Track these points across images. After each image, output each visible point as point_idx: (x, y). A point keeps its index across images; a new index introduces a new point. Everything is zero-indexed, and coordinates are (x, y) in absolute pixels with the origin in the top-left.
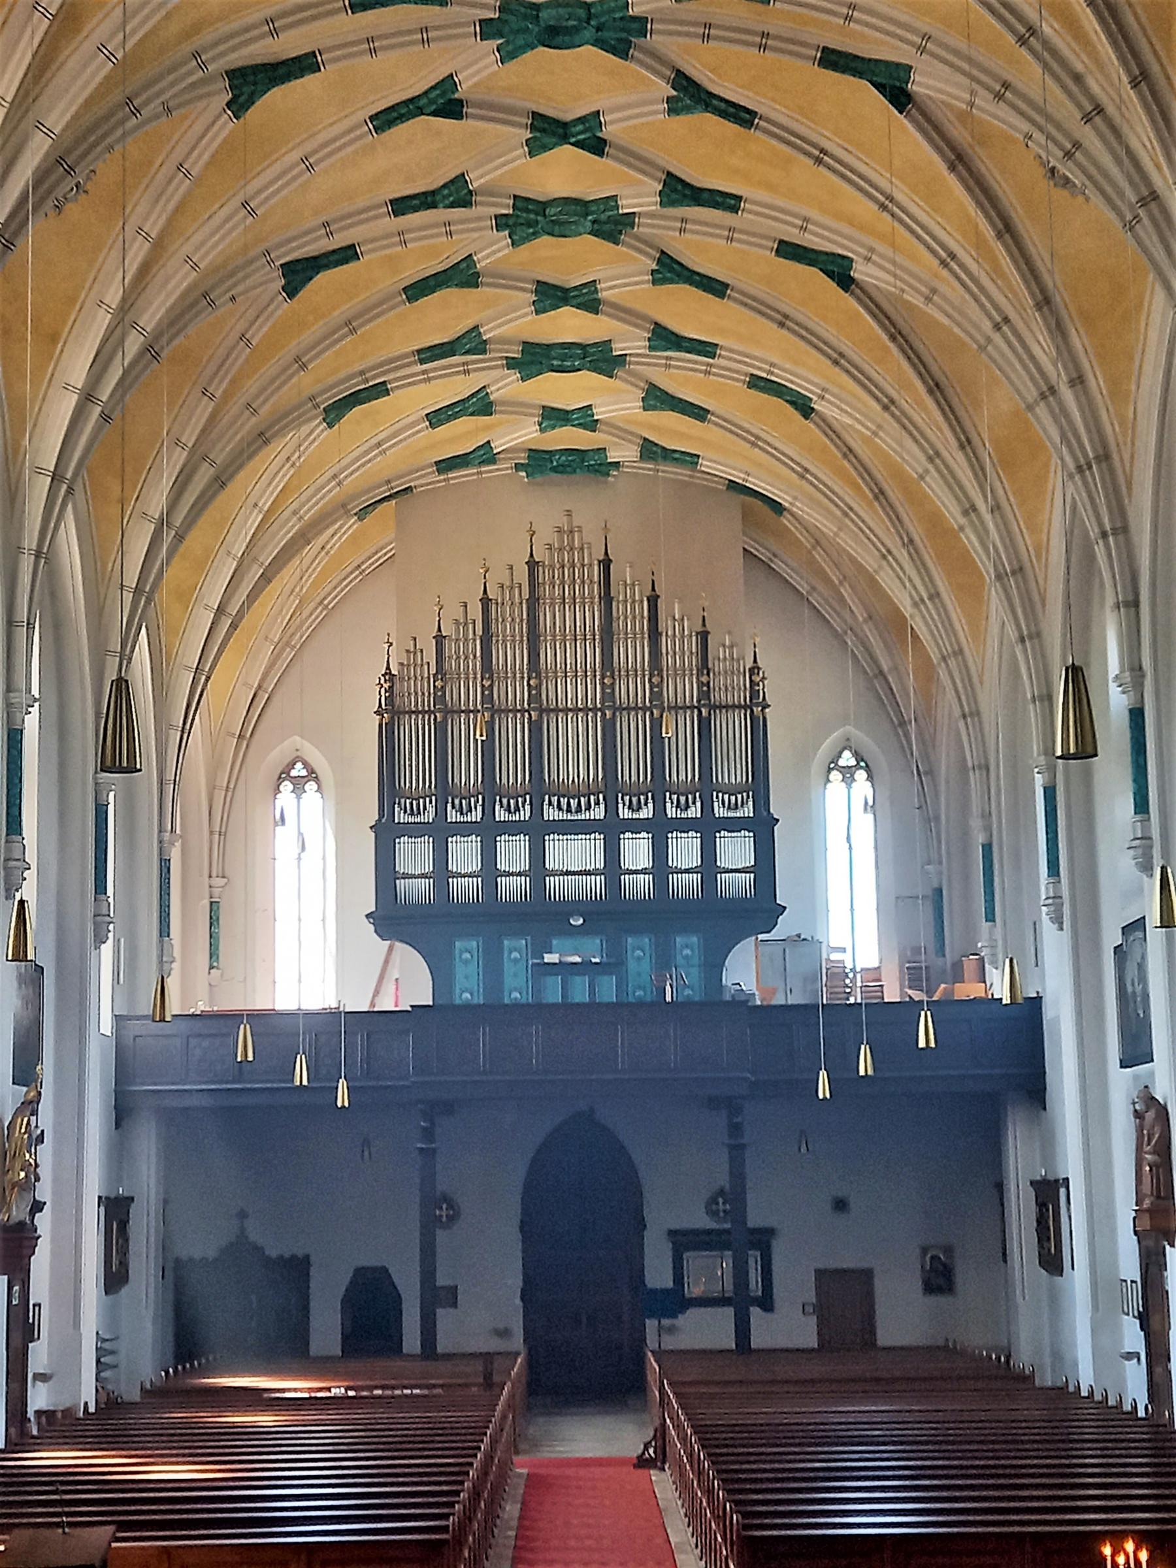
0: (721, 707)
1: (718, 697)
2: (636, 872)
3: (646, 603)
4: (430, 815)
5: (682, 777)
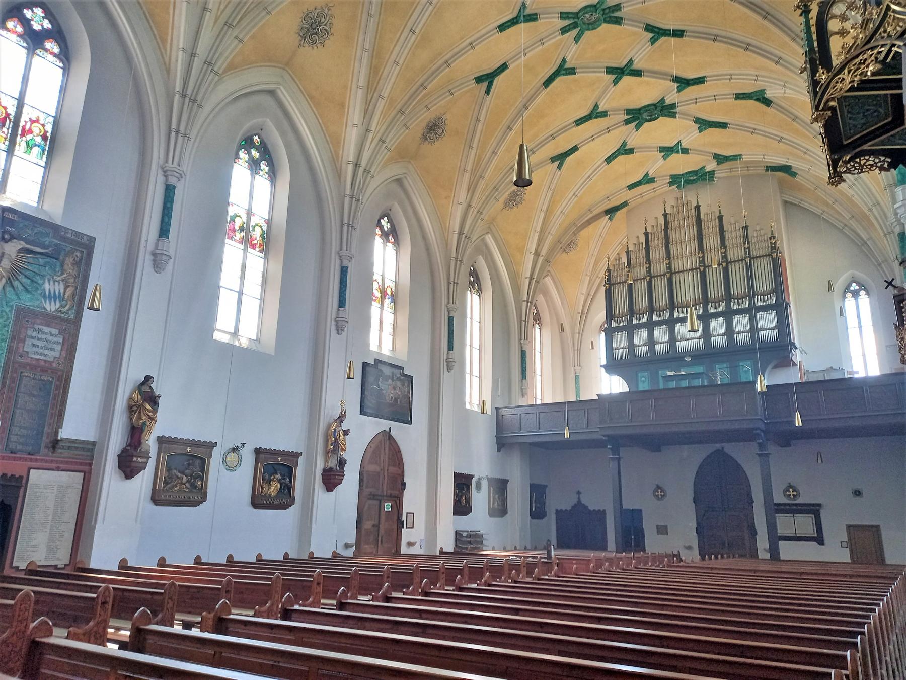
0: (756, 257)
1: (753, 254)
2: (718, 336)
3: (717, 220)
4: (625, 323)
5: (740, 291)
